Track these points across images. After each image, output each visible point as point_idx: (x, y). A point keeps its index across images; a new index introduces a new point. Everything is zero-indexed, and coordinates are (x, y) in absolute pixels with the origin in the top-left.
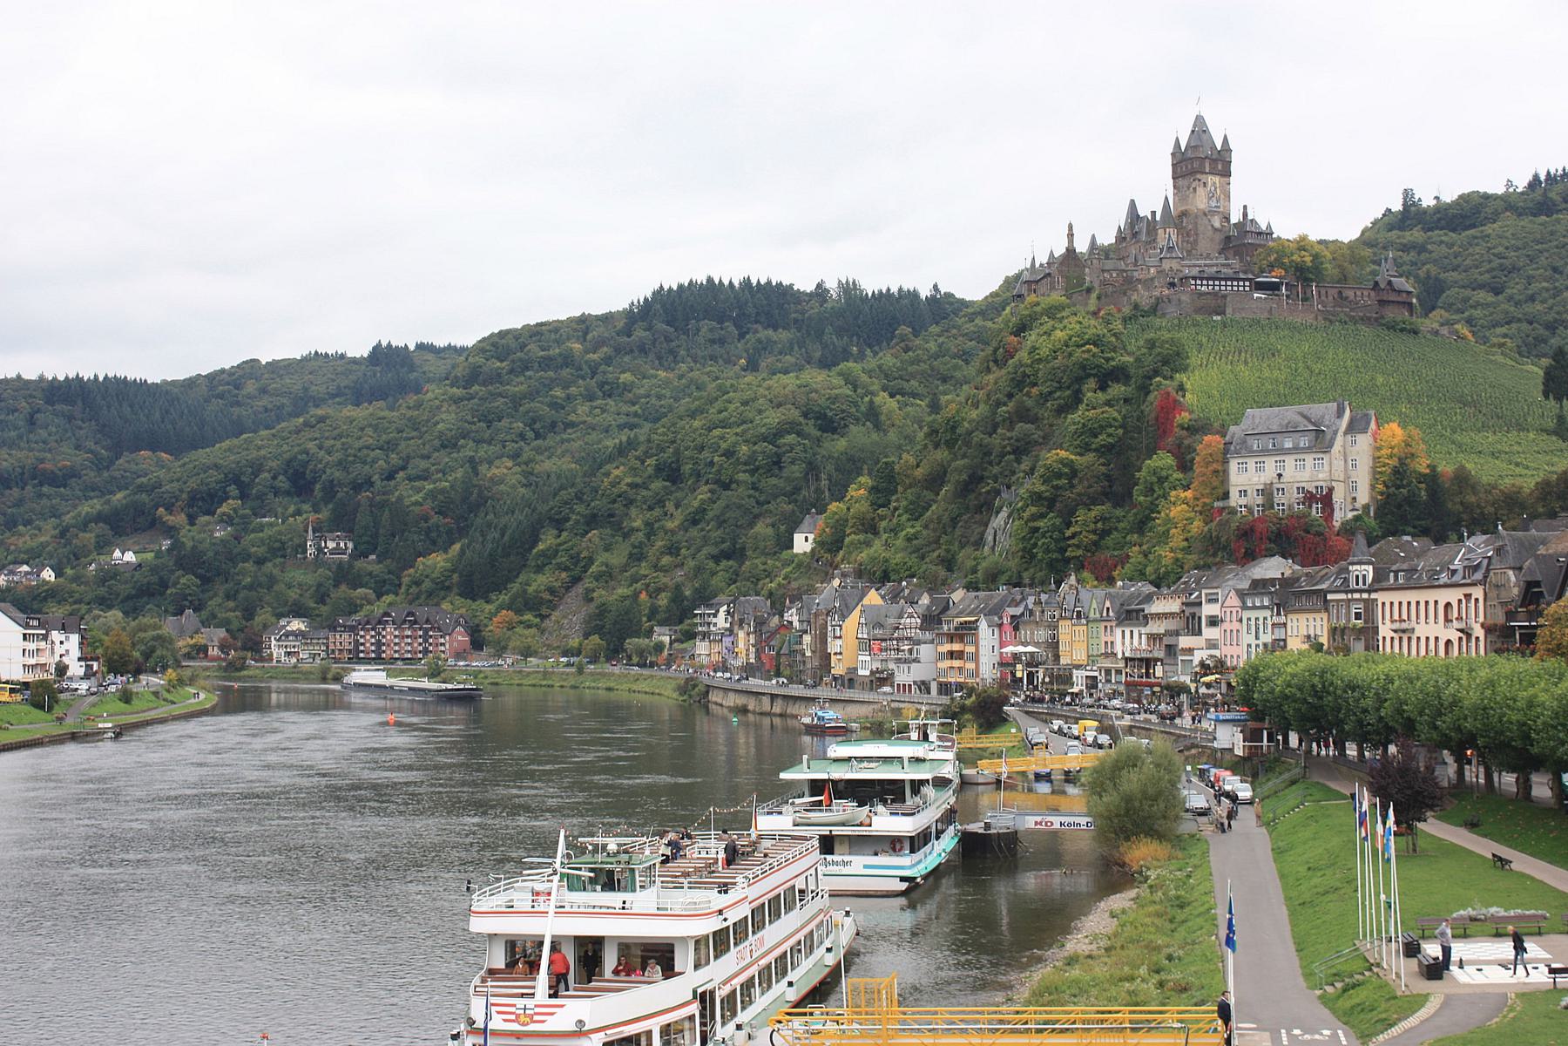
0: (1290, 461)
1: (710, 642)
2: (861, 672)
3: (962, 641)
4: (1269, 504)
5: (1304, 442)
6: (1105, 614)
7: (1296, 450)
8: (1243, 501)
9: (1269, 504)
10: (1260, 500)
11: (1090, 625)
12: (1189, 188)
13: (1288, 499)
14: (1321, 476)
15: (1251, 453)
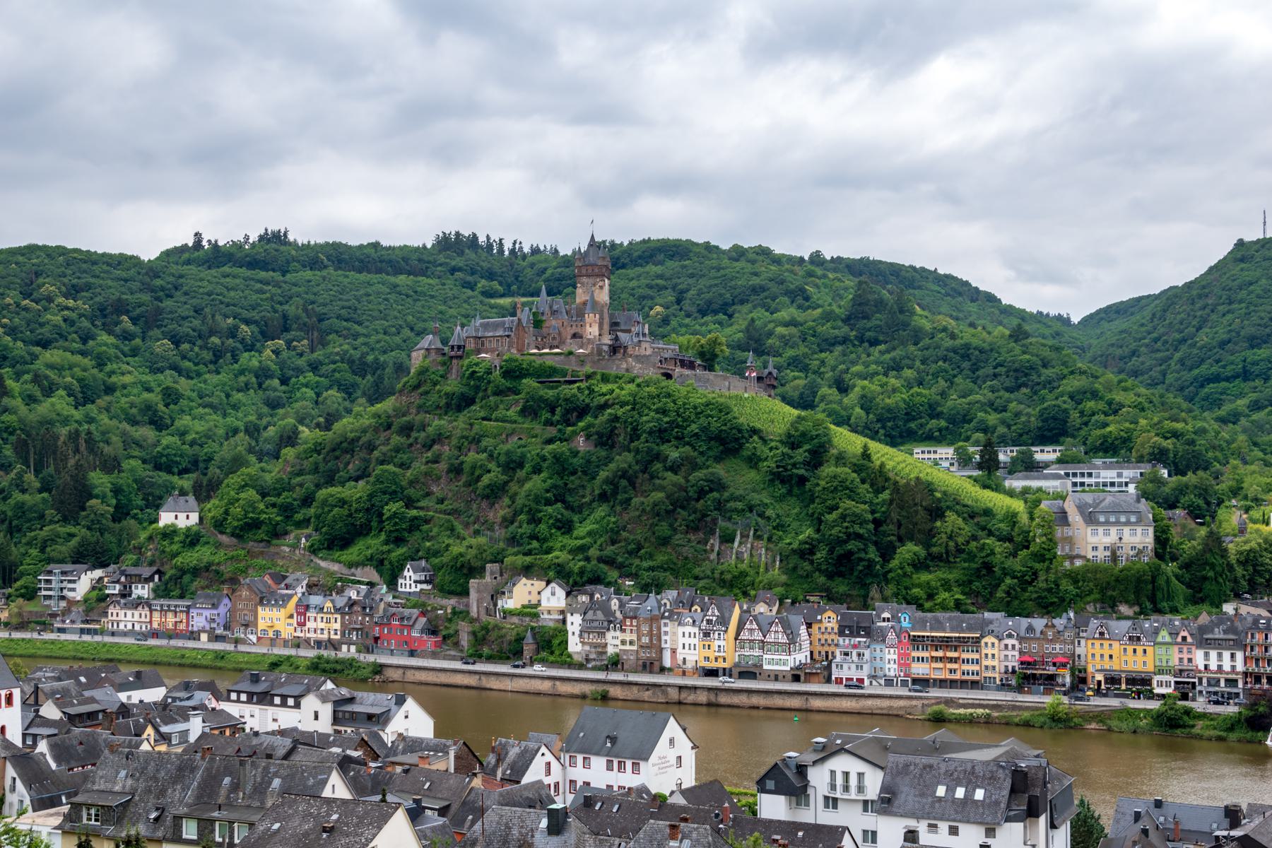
0: (1126, 530)
1: (151, 611)
2: (766, 667)
3: (956, 651)
4: (1114, 557)
5: (1133, 519)
6: (1179, 639)
7: (1128, 523)
8: (1095, 553)
9: (1114, 557)
10: (1108, 553)
11: (1157, 647)
12: (594, 285)
13: (1126, 553)
14: (1147, 540)
15: (1099, 523)
